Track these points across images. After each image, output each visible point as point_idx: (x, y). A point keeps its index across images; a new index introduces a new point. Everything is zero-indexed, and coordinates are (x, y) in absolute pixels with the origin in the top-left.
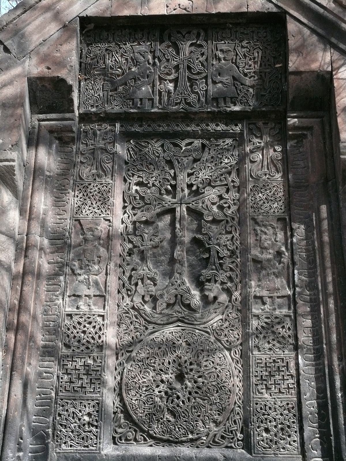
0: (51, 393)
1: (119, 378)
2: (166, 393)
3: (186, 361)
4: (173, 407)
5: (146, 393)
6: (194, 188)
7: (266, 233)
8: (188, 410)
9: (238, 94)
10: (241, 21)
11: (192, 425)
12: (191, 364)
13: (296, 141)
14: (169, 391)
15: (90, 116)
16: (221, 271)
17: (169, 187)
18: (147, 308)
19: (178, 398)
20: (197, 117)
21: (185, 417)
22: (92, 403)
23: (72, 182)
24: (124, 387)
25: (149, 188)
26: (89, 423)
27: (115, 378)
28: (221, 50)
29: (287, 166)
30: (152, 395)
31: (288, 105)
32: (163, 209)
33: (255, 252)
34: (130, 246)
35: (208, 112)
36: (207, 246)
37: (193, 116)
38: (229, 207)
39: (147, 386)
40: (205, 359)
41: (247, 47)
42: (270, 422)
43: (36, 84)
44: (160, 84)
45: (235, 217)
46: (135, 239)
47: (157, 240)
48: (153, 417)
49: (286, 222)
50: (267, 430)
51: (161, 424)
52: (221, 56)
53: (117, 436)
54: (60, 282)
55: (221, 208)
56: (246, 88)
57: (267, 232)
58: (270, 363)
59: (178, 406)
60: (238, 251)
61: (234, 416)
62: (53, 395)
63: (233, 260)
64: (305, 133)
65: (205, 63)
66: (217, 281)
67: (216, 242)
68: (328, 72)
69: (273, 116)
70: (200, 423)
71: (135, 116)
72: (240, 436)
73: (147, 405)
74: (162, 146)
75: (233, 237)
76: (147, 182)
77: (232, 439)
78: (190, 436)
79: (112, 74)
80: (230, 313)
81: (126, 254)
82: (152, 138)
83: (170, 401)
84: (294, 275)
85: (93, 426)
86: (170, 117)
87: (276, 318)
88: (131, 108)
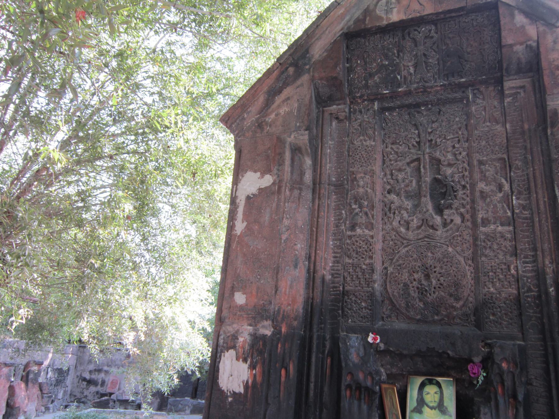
0: (339, 287)
1: (384, 277)
2: (418, 288)
3: (431, 266)
6: (433, 142)
7: (489, 171)
9: (463, 69)
10: (462, 13)
12: (435, 267)
13: (511, 98)
14: (419, 286)
16: (456, 201)
17: (415, 143)
18: (403, 230)
19: (426, 291)
20: (433, 90)
23: (347, 146)
24: (388, 284)
25: (401, 145)
26: (365, 308)
28: (449, 38)
29: (505, 118)
31: (504, 71)
32: (411, 159)
33: (481, 186)
34: (388, 187)
35: (441, 86)
36: (445, 183)
37: (429, 90)
38: (460, 153)
40: (445, 264)
41: (468, 32)
42: (496, 308)
44: (404, 69)
45: (465, 160)
46: (392, 181)
47: (407, 181)
49: (505, 161)
50: (494, 314)
52: (448, 42)
53: (385, 316)
54: (342, 214)
55: (455, 155)
57: (490, 169)
58: (495, 266)
60: (468, 186)
62: (341, 289)
63: (464, 191)
64: (519, 91)
65: (437, 50)
67: (450, 180)
69: (493, 81)
74: (409, 114)
75: (464, 175)
76: (398, 141)
77: (467, 320)
79: (370, 68)
80: (464, 231)
81: (386, 192)
84: (512, 200)
85: (368, 309)
87: (500, 233)
88: (385, 90)
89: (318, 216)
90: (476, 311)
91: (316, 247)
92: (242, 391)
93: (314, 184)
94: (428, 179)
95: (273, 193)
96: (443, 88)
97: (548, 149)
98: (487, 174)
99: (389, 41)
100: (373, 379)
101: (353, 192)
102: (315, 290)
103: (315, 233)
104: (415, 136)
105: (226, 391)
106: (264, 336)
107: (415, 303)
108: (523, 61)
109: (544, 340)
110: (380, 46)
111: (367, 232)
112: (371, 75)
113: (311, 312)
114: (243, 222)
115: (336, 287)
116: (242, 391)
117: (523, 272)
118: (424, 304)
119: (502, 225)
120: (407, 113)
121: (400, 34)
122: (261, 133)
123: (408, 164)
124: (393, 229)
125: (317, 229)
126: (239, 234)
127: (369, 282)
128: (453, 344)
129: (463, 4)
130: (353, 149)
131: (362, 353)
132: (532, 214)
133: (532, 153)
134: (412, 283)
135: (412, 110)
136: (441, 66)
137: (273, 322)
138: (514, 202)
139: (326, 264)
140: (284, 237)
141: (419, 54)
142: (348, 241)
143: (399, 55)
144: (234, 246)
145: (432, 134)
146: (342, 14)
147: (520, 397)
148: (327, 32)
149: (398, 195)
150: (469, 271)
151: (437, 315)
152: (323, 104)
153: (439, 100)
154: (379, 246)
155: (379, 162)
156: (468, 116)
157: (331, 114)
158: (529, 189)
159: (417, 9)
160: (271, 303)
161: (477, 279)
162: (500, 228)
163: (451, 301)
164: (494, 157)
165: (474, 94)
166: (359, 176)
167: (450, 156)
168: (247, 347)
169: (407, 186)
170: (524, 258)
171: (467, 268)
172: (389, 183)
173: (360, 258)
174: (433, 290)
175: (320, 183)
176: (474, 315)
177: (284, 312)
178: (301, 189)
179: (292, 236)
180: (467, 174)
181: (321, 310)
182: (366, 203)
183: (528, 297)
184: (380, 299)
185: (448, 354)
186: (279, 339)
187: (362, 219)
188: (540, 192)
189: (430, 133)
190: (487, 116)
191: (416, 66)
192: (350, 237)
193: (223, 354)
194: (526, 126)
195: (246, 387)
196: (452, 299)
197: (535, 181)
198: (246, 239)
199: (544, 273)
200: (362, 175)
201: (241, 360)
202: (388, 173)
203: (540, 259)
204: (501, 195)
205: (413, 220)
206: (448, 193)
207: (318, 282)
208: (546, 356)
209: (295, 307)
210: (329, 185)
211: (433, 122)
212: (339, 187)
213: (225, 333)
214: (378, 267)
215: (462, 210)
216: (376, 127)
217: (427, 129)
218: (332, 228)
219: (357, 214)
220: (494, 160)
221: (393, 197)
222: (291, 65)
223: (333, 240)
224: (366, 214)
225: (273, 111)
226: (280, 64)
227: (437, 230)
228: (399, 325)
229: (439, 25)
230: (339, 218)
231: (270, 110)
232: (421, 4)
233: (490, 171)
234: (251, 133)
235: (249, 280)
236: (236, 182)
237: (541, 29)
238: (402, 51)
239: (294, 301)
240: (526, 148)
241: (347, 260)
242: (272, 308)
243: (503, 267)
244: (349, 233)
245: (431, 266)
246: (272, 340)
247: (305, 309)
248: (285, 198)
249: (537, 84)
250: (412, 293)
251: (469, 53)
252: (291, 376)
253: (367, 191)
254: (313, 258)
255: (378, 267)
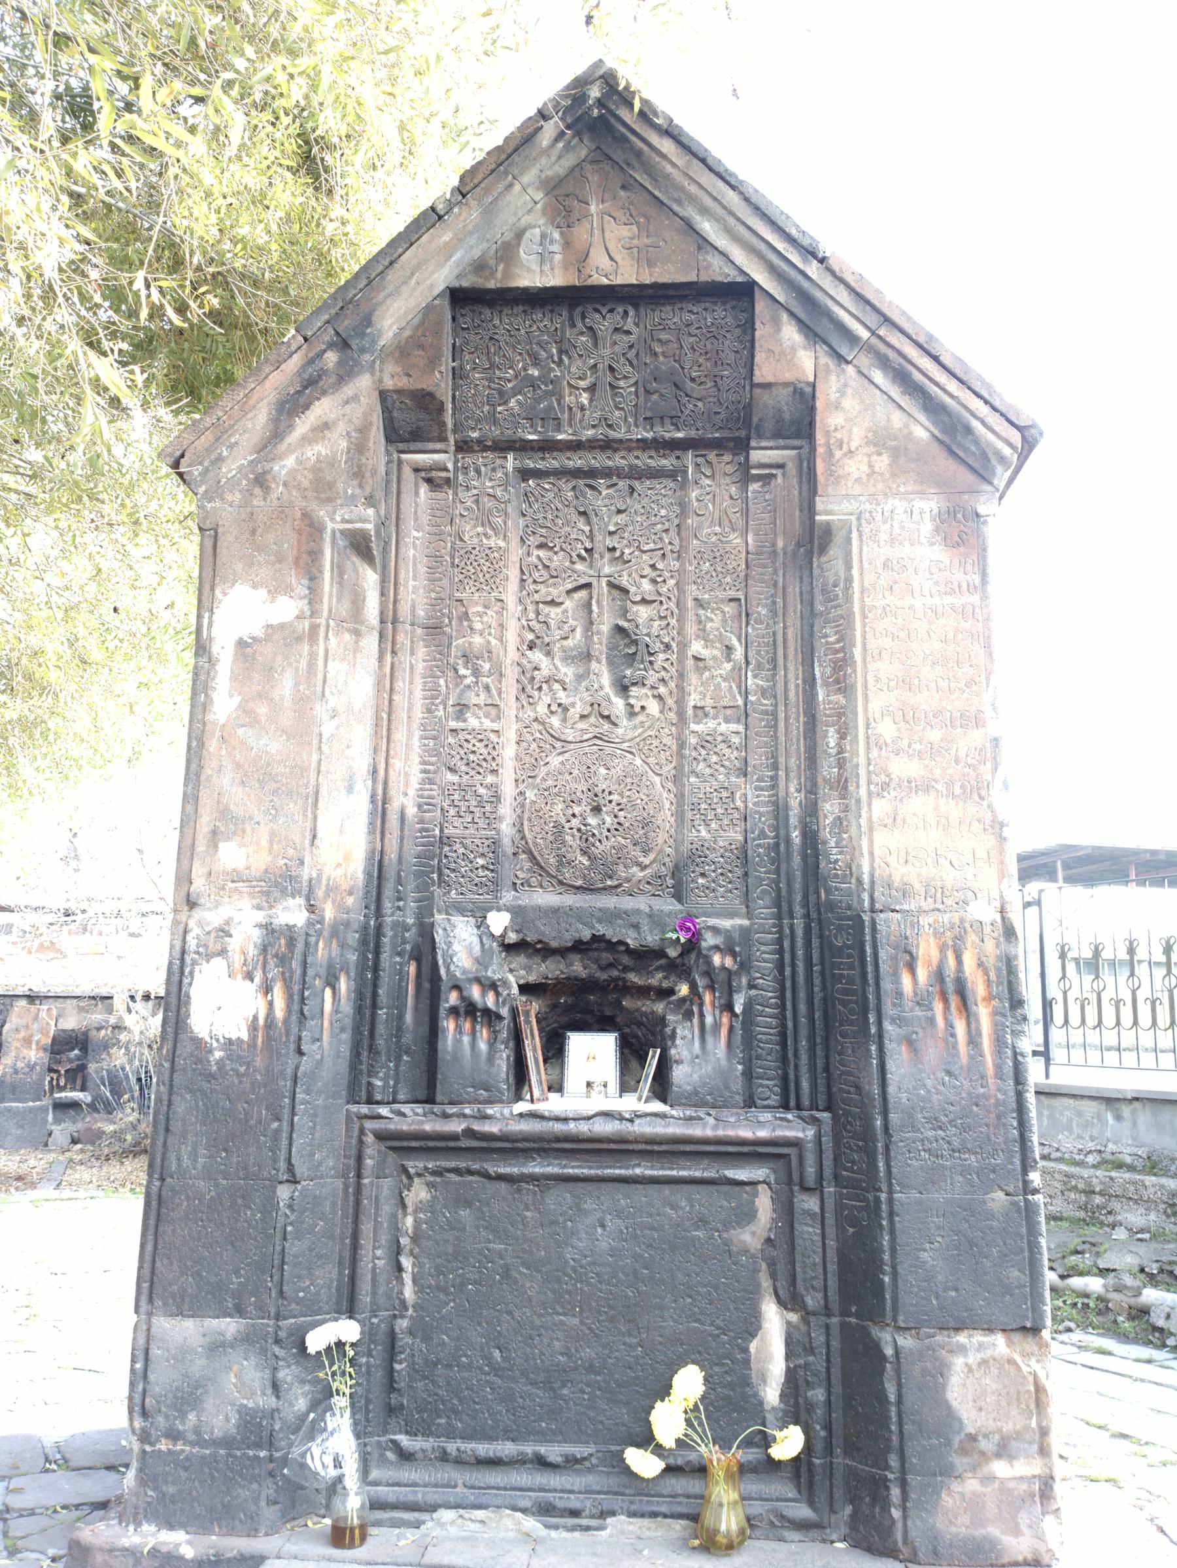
1: (519, 811)
2: (579, 830)
6: (618, 554)
17: (583, 552)
18: (555, 721)
22: (487, 842)
24: (526, 823)
28: (659, 340)
32: (575, 584)
34: (530, 636)
47: (566, 628)
50: (703, 875)
52: (658, 349)
55: (654, 581)
56: (693, 401)
60: (674, 645)
62: (437, 832)
65: (635, 362)
67: (645, 631)
68: (808, 383)
69: (731, 444)
70: (621, 867)
72: (670, 882)
78: (609, 883)
89: (392, 689)
90: (677, 871)
91: (388, 751)
92: (245, 1036)
93: (382, 622)
94: (605, 628)
95: (299, 639)
97: (812, 593)
98: (709, 625)
99: (543, 323)
100: (498, 994)
101: (460, 641)
102: (388, 836)
103: (385, 723)
104: (583, 538)
105: (208, 1039)
106: (290, 928)
108: (787, 416)
109: (779, 917)
110: (523, 332)
111: (488, 724)
112: (504, 397)
113: (380, 877)
114: (231, 696)
115: (427, 830)
116: (245, 1036)
117: (755, 804)
119: (727, 720)
120: (570, 486)
121: (565, 313)
122: (265, 499)
123: (569, 592)
124: (536, 720)
125: (389, 715)
126: (222, 722)
127: (491, 820)
128: (636, 927)
129: (692, 277)
130: (462, 552)
131: (477, 949)
132: (776, 705)
133: (784, 596)
135: (581, 482)
136: (642, 399)
137: (308, 900)
138: (749, 682)
139: (407, 785)
140: (327, 731)
141: (600, 366)
142: (451, 740)
143: (561, 360)
144: (212, 745)
145: (616, 537)
146: (447, 243)
147: (738, 1009)
148: (413, 281)
149: (548, 654)
150: (667, 801)
151: (611, 878)
152: (401, 446)
153: (631, 466)
154: (509, 752)
155: (513, 586)
156: (683, 505)
157: (417, 470)
158: (774, 661)
159: (601, 266)
160: (302, 863)
161: (680, 815)
162: (724, 727)
163: (636, 853)
164: (721, 594)
165: (698, 465)
166: (472, 610)
167: (646, 585)
168: (252, 951)
169: (566, 638)
170: (758, 780)
171: (665, 795)
172: (531, 630)
173: (473, 773)
174: (605, 833)
175: (395, 621)
176: (673, 876)
177: (329, 879)
178: (357, 633)
179: (342, 730)
180: (673, 622)
181: (399, 876)
182: (487, 666)
183: (759, 846)
184: (509, 850)
185: (627, 944)
186: (319, 934)
187: (477, 698)
188: (791, 667)
189: (611, 533)
190: (716, 515)
191: (592, 389)
192: (454, 731)
193: (197, 968)
194: (780, 544)
195: (253, 1027)
196: (638, 848)
197: (785, 648)
198: (241, 731)
199: (787, 807)
200: (480, 609)
201: (239, 976)
202: (531, 608)
203: (782, 784)
204: (728, 666)
205: (573, 705)
206: (638, 657)
207: (393, 820)
208: (780, 941)
209: (350, 870)
210: (412, 624)
211: (619, 512)
212: (434, 630)
213: (200, 924)
214: (508, 790)
215: (662, 690)
216: (509, 510)
217: (607, 525)
218: (418, 713)
219: (469, 687)
220: (722, 601)
221: (537, 656)
222: (331, 346)
223: (422, 738)
224: (487, 688)
225: (290, 450)
226: (306, 339)
227: (615, 725)
228: (545, 898)
229: (642, 310)
230: (432, 694)
231: (282, 447)
232: (611, 259)
233: (714, 623)
234: (238, 495)
235: (251, 818)
236: (205, 603)
237: (825, 360)
238: (567, 352)
239: (347, 858)
240: (775, 585)
241: (451, 777)
242: (306, 872)
243: (725, 794)
244: (453, 724)
246: (307, 934)
247: (368, 874)
248: (327, 652)
249: (805, 465)
250: (568, 838)
251: (693, 380)
252: (343, 1001)
253: (489, 643)
254: (382, 773)
255: (508, 790)
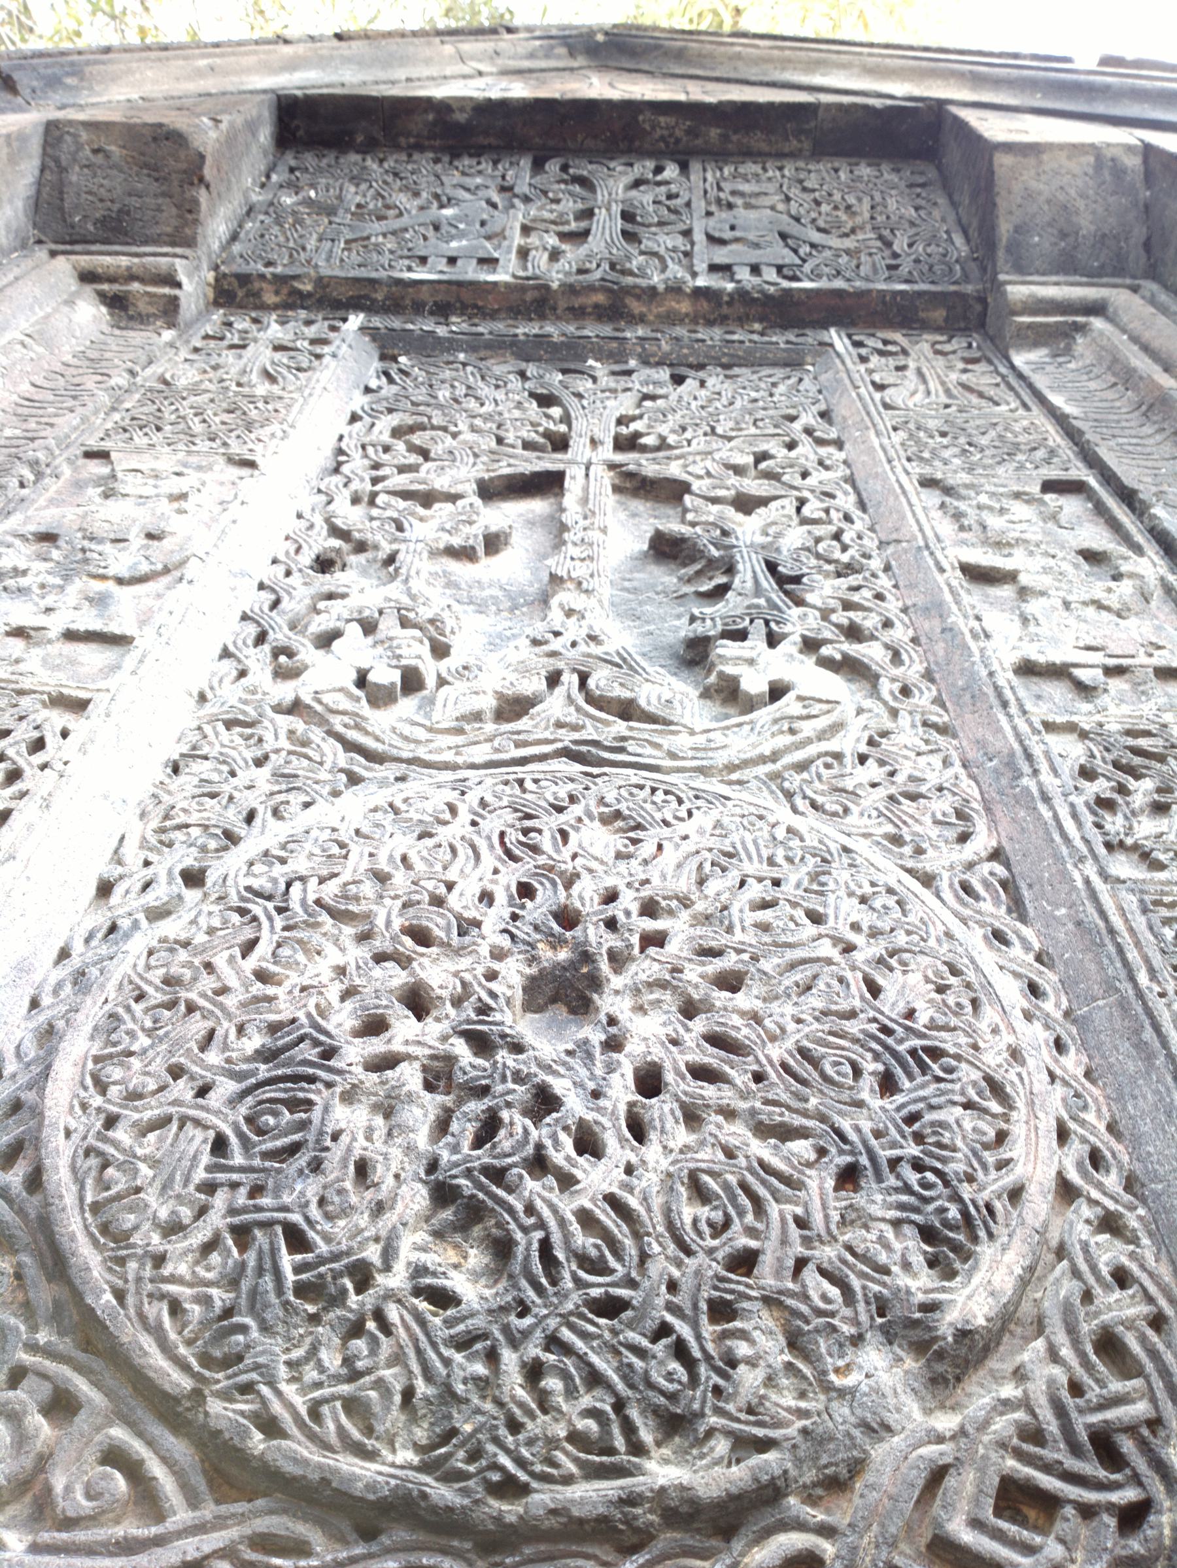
4: (487, 1171)
5: (253, 1073)
8: (633, 1202)
11: (680, 1351)
15: (257, 285)
21: (597, 1267)
27: (35, 1004)
30: (312, 1080)
35: (698, 292)
37: (636, 307)
39: (274, 1028)
43: (76, 143)
48: (274, 1252)
51: (356, 1329)
59: (539, 1164)
61: (1087, 1297)
66: (784, 636)
69: (939, 315)
71: (425, 294)
73: (238, 1159)
82: (482, 354)
83: (464, 1129)
86: (554, 309)
96: (704, 305)
107: (373, 1253)
108: (1086, 224)
118: (502, 1248)
134: (375, 1026)
229: (695, 167)
245: (611, 897)
